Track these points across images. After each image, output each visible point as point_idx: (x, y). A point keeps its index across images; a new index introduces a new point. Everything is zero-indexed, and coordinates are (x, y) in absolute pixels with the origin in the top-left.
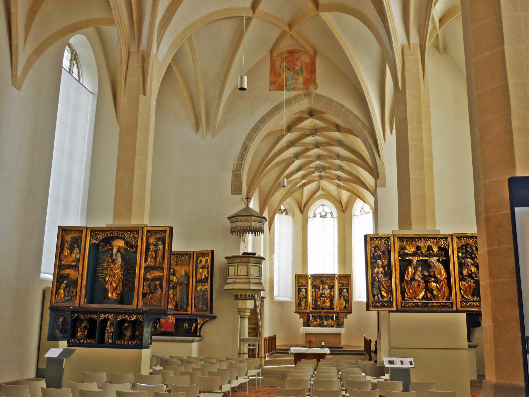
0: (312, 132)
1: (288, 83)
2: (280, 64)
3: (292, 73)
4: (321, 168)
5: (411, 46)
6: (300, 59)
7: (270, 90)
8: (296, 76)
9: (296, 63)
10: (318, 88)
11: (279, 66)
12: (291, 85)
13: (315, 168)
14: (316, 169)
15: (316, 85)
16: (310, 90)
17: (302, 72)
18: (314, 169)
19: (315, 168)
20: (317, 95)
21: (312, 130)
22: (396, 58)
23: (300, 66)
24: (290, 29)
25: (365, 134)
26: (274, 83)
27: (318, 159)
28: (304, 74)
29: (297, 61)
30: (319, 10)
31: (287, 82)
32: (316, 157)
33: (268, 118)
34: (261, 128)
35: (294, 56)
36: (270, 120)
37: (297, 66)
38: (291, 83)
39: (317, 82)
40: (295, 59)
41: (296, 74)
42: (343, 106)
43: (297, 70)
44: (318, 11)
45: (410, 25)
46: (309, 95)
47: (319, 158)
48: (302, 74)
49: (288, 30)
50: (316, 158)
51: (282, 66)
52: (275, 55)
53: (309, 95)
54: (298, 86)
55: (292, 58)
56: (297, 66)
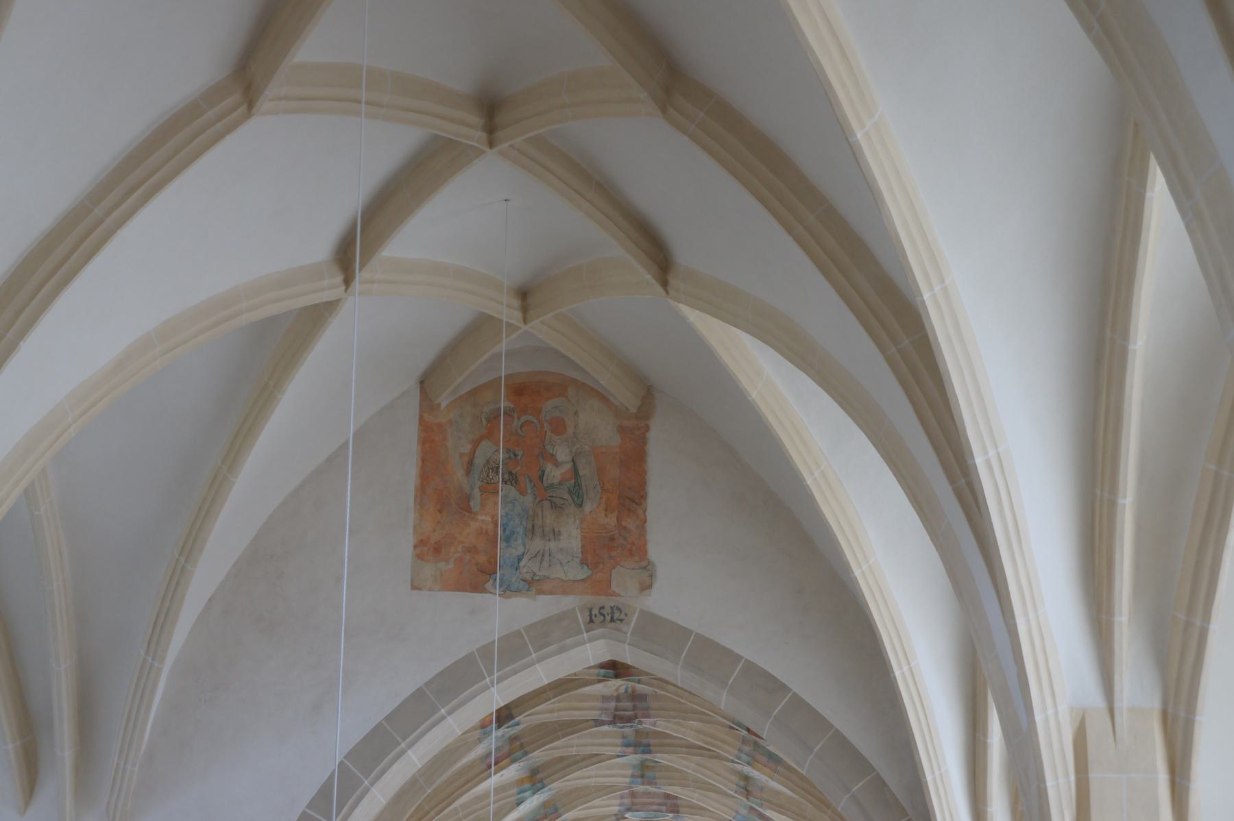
0: (616, 709)
2: (468, 448)
3: (529, 499)
4: (657, 800)
5: (1122, 719)
6: (570, 430)
7: (414, 587)
8: (549, 518)
10: (656, 586)
11: (466, 459)
12: (522, 564)
13: (627, 801)
14: (633, 804)
15: (645, 568)
17: (577, 493)
18: (621, 805)
19: (627, 801)
21: (618, 699)
22: (1050, 783)
23: (569, 466)
24: (525, 310)
26: (437, 549)
27: (642, 776)
28: (588, 507)
30: (673, 281)
33: (404, 739)
34: (367, 790)
36: (410, 746)
37: (557, 464)
39: (653, 553)
40: (546, 425)
41: (547, 504)
43: (551, 486)
44: (667, 292)
45: (1117, 619)
46: (612, 620)
47: (649, 774)
48: (580, 505)
50: (633, 776)
51: (476, 461)
52: (444, 401)
54: (558, 573)
55: (531, 418)
56: (557, 464)
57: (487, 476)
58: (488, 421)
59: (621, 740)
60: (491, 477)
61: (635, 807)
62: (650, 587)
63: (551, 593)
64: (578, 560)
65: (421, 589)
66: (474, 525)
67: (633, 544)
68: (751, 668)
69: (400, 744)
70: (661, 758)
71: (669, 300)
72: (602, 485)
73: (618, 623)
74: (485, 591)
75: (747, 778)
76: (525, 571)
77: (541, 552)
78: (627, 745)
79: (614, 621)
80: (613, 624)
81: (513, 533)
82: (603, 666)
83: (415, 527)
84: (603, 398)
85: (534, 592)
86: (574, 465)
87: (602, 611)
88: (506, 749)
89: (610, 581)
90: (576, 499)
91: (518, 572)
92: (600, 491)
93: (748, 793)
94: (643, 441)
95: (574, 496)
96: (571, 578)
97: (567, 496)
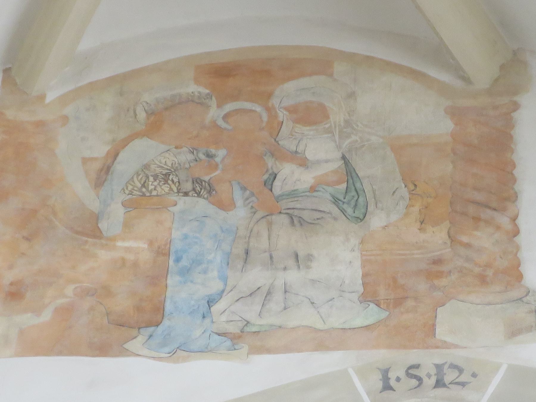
12: (217, 308)
16: (446, 345)
29: (300, 128)
31: (172, 280)
38: (221, 294)
40: (282, 115)
46: (439, 384)
48: (361, 219)
58: (150, 114)
64: (355, 297)
67: (488, 266)
72: (412, 187)
73: (455, 391)
74: (124, 352)
76: (224, 318)
77: (265, 290)
79: (444, 385)
80: (440, 391)
81: (197, 262)
87: (412, 371)
89: (434, 325)
90: (349, 210)
91: (207, 321)
92: (407, 195)
95: (345, 206)
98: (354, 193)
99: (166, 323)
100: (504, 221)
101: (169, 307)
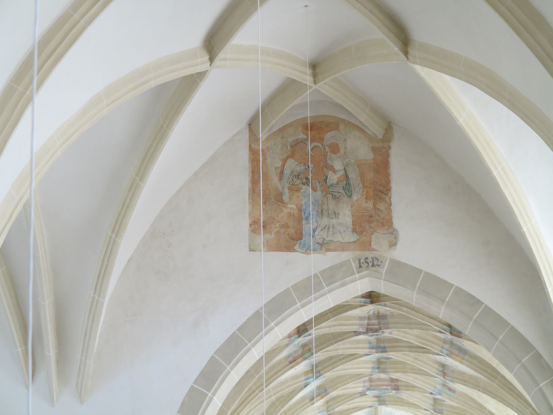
0: (368, 325)
1: (309, 226)
2: (279, 164)
3: (319, 193)
4: (385, 383)
6: (342, 151)
7: (251, 250)
8: (331, 205)
9: (330, 162)
10: (399, 244)
11: (279, 171)
12: (316, 233)
13: (367, 384)
14: (371, 386)
16: (374, 250)
17: (348, 189)
18: (364, 386)
19: (367, 384)
20: (397, 265)
21: (369, 318)
23: (342, 172)
24: (315, 75)
25: (545, 389)
27: (378, 368)
28: (355, 198)
30: (411, 51)
31: (304, 222)
32: (374, 362)
33: (250, 341)
34: (229, 373)
35: (322, 140)
36: (253, 345)
37: (334, 171)
39: (397, 223)
40: (327, 148)
41: (330, 196)
42: (476, 302)
43: (332, 185)
44: (407, 58)
46: (373, 266)
47: (382, 366)
48: (350, 197)
49: (308, 79)
50: (373, 368)
51: (285, 172)
53: (373, 266)
54: (338, 238)
55: (317, 144)
56: (334, 171)
57: (293, 181)
58: (292, 147)
59: (369, 345)
60: (295, 181)
61: (373, 388)
62: (395, 244)
63: (335, 250)
64: (350, 230)
65: (255, 251)
66: (286, 211)
67: (384, 219)
68: (459, 291)
69: (247, 344)
70: (392, 355)
71: (408, 63)
72: (363, 184)
73: (377, 268)
74: (294, 250)
75: (443, 366)
76: (318, 237)
77: (328, 226)
78: (372, 348)
80: (373, 268)
82: (363, 296)
83: (250, 214)
84: (361, 129)
85: (324, 250)
86: (346, 171)
88: (300, 352)
89: (371, 242)
92: (362, 187)
93: (444, 374)
94: (388, 156)
95: (346, 191)
96: (347, 241)
97: (342, 191)
98: (348, 186)
99: (304, 238)
100: (387, 199)
101: (304, 233)
